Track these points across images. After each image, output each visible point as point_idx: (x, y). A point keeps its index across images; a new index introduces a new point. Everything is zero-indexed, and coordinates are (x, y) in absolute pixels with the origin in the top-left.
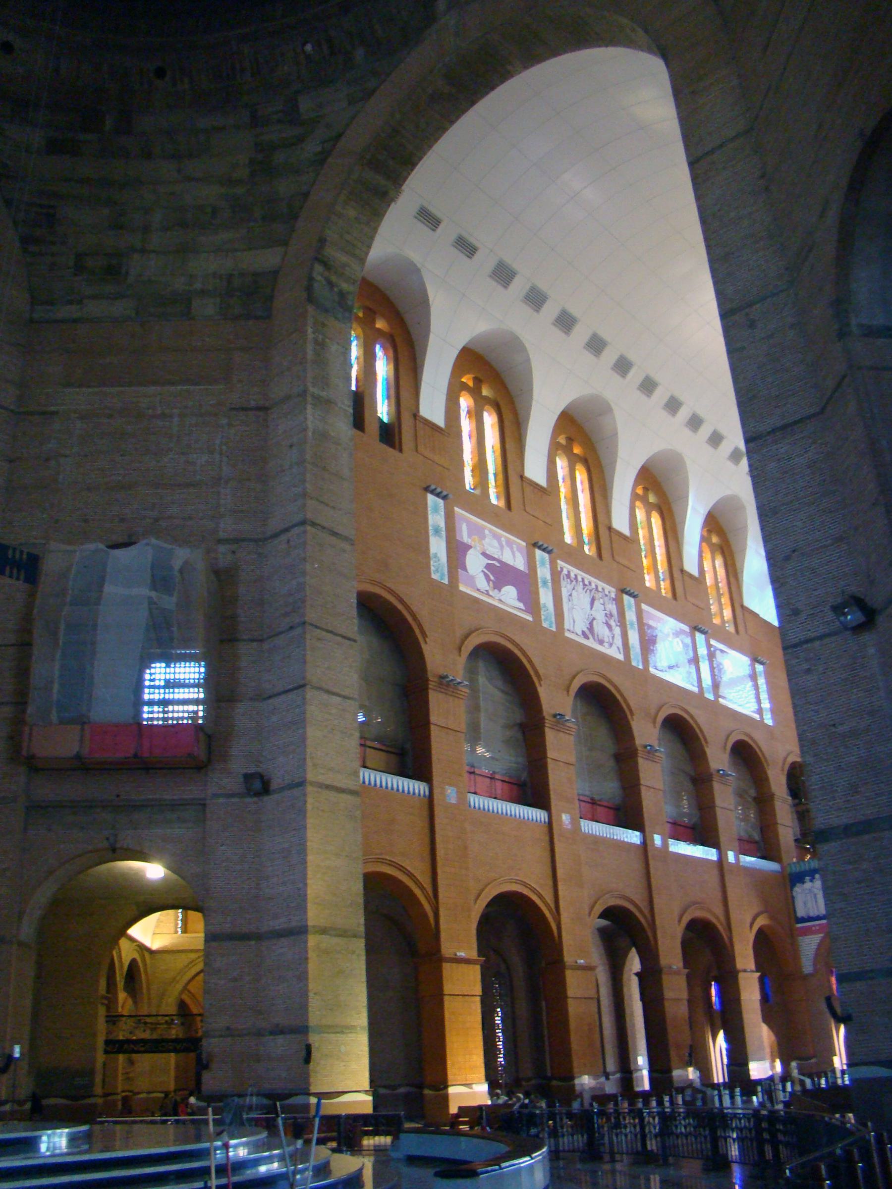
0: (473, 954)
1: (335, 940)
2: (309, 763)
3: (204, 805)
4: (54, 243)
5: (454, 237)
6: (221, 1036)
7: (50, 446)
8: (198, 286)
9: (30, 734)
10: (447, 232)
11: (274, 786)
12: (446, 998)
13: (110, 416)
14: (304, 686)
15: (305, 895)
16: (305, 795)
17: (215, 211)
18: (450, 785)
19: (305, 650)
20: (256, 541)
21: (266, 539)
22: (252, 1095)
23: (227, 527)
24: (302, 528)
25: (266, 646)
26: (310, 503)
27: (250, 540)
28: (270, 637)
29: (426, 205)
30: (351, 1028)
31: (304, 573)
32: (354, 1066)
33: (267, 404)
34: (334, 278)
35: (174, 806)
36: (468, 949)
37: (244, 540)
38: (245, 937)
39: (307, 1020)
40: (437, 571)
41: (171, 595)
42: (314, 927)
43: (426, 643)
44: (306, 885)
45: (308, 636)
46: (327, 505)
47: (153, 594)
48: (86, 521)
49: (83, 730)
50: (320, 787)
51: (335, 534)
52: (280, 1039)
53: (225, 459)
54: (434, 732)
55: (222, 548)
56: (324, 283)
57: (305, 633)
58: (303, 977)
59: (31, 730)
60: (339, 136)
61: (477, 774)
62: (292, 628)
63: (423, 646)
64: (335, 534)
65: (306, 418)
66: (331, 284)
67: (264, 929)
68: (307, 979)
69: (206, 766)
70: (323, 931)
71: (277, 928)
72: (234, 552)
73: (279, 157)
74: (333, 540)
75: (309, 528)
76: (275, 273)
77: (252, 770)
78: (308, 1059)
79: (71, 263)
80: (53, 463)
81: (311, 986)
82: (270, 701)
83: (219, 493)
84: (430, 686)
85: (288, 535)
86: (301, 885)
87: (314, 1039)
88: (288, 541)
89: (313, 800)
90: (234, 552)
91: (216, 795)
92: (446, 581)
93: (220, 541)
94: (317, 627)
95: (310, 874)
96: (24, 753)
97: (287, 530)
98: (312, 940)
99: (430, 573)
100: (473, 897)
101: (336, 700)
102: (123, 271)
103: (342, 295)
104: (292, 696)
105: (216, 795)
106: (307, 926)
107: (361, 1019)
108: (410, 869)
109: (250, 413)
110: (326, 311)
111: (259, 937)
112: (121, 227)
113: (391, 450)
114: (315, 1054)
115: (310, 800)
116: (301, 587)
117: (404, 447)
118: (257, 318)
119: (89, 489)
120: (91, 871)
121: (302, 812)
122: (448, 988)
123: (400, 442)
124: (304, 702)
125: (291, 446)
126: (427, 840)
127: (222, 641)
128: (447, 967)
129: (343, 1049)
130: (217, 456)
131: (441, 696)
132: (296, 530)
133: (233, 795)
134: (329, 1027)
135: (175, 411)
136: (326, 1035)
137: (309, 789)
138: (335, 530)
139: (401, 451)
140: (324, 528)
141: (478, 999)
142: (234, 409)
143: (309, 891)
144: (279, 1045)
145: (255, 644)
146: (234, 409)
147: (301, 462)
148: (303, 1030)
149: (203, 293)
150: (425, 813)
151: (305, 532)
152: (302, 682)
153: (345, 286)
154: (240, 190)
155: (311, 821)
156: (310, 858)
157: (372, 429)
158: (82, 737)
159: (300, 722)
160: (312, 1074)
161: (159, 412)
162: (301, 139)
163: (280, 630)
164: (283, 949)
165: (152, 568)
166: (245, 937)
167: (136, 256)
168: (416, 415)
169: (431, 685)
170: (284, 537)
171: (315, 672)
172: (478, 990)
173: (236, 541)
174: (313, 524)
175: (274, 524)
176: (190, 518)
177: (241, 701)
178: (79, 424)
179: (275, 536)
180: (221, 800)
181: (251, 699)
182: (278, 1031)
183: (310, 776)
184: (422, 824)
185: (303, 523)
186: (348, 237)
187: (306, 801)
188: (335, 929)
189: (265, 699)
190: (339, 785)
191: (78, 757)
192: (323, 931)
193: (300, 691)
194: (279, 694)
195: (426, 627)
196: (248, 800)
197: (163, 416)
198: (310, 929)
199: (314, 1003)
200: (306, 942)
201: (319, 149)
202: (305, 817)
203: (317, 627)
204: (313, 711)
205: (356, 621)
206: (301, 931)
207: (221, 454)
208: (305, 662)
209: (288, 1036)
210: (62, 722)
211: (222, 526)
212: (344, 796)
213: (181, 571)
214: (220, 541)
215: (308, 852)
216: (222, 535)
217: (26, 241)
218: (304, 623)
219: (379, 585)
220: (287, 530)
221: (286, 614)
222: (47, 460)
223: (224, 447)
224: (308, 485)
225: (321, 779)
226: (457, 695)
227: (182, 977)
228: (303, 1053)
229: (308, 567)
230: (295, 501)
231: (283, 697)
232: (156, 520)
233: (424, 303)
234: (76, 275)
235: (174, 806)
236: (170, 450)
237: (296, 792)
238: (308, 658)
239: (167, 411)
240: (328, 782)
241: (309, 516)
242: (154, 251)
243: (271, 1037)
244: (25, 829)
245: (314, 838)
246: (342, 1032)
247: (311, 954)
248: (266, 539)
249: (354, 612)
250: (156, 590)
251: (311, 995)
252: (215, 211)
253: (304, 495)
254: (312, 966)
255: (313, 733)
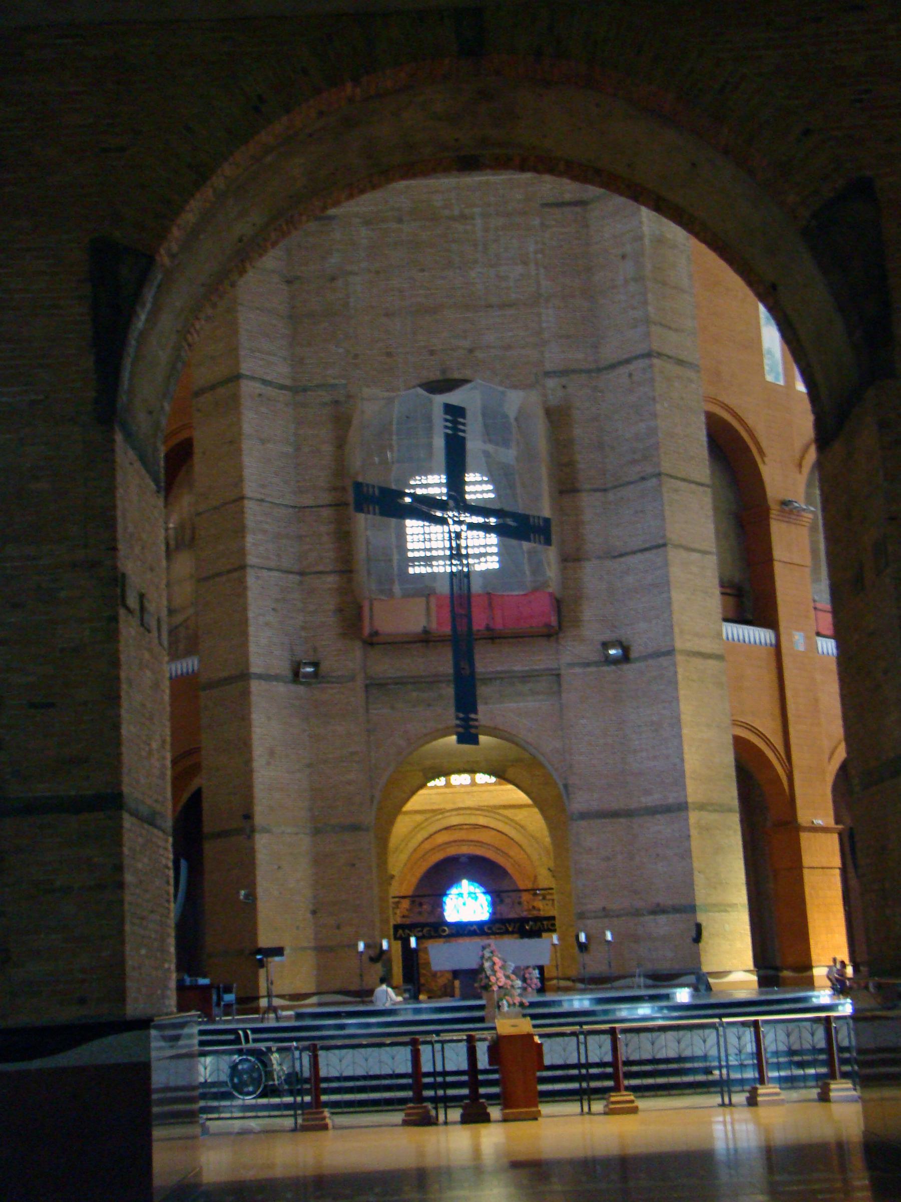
0: (830, 821)
1: (714, 816)
2: (676, 630)
3: (558, 675)
6: (596, 918)
7: (333, 261)
9: (371, 609)
11: (633, 654)
12: (806, 872)
13: (400, 221)
14: (664, 545)
15: (684, 771)
16: (675, 665)
18: (798, 630)
19: (662, 505)
20: (589, 371)
21: (599, 370)
22: (639, 976)
23: (554, 357)
24: (647, 361)
25: (611, 496)
26: (654, 329)
27: (581, 371)
28: (615, 487)
30: (733, 906)
31: (654, 415)
32: (738, 945)
35: (526, 677)
36: (824, 817)
37: (574, 371)
38: (615, 814)
39: (694, 899)
40: (771, 370)
41: (506, 443)
42: (693, 803)
43: (764, 462)
44: (682, 760)
45: (664, 489)
46: (670, 328)
47: (490, 447)
48: (389, 355)
49: (428, 603)
50: (688, 655)
51: (681, 362)
52: (662, 919)
53: (542, 271)
54: (779, 570)
55: (551, 383)
57: (660, 485)
58: (686, 855)
59: (371, 605)
61: (821, 610)
62: (643, 479)
63: (761, 467)
64: (681, 362)
65: (641, 222)
67: (633, 805)
68: (691, 857)
69: (557, 634)
70: (702, 807)
71: (649, 804)
72: (564, 387)
74: (677, 370)
75: (655, 361)
77: (607, 636)
78: (698, 938)
80: (340, 283)
81: (695, 865)
82: (623, 559)
83: (539, 315)
84: (772, 516)
85: (631, 367)
86: (677, 761)
87: (701, 918)
88: (630, 375)
89: (685, 669)
90: (564, 387)
91: (571, 665)
92: (781, 382)
93: (548, 374)
94: (671, 477)
95: (686, 748)
96: (367, 631)
97: (627, 361)
98: (693, 817)
99: (763, 375)
100: (827, 756)
101: (695, 556)
104: (648, 555)
105: (571, 665)
106: (686, 803)
107: (740, 896)
108: (761, 730)
109: (567, 210)
111: (629, 814)
114: (705, 934)
115: (680, 670)
116: (652, 432)
119: (387, 315)
120: (428, 747)
121: (673, 683)
122: (807, 860)
124: (666, 564)
125: (624, 257)
126: (776, 694)
127: (561, 492)
128: (804, 836)
129: (727, 927)
130: (532, 266)
131: (784, 526)
132: (641, 363)
133: (588, 665)
134: (715, 905)
135: (475, 210)
136: (710, 914)
137: (679, 658)
138: (680, 357)
140: (669, 357)
141: (838, 872)
142: (547, 205)
143: (687, 767)
144: (662, 925)
145: (598, 494)
146: (547, 205)
147: (639, 279)
148: (691, 909)
150: (773, 664)
151: (651, 366)
152: (661, 542)
155: (682, 692)
156: (685, 731)
158: (428, 608)
159: (663, 585)
160: (702, 954)
161: (456, 213)
163: (627, 479)
164: (659, 827)
165: (484, 415)
166: (615, 814)
169: (774, 513)
170: (623, 370)
171: (675, 530)
172: (837, 862)
173: (564, 373)
174: (659, 355)
175: (609, 353)
176: (509, 347)
177: (588, 560)
178: (364, 232)
179: (613, 367)
180: (578, 670)
181: (599, 558)
182: (658, 910)
183: (679, 644)
184: (770, 677)
185: (649, 355)
187: (676, 672)
188: (712, 804)
189: (615, 557)
190: (703, 650)
191: (426, 631)
192: (702, 807)
193: (660, 550)
194: (634, 552)
195: (764, 444)
196: (606, 668)
197: (463, 217)
198: (690, 806)
199: (699, 880)
200: (687, 819)
202: (676, 689)
203: (671, 477)
204: (676, 572)
205: (707, 463)
206: (682, 807)
207: (537, 264)
208: (663, 519)
209: (671, 916)
210: (407, 595)
211: (547, 355)
212: (711, 663)
213: (516, 419)
214: (548, 374)
215: (683, 725)
216: (548, 367)
218: (659, 475)
219: (714, 401)
220: (627, 361)
221: (634, 462)
222: (333, 279)
223: (540, 256)
224: (650, 308)
225: (688, 646)
226: (798, 522)
227: (407, 844)
228: (693, 934)
229: (658, 407)
230: (636, 327)
231: (639, 556)
232: (471, 351)
235: (526, 677)
236: (475, 262)
237: (664, 661)
238: (667, 514)
239: (466, 211)
240: (696, 648)
241: (655, 346)
243: (652, 917)
244: (367, 710)
245: (687, 709)
246: (726, 911)
247: (694, 832)
248: (599, 370)
249: (705, 453)
250: (490, 441)
251: (696, 873)
253: (647, 321)
254: (695, 843)
255: (677, 596)
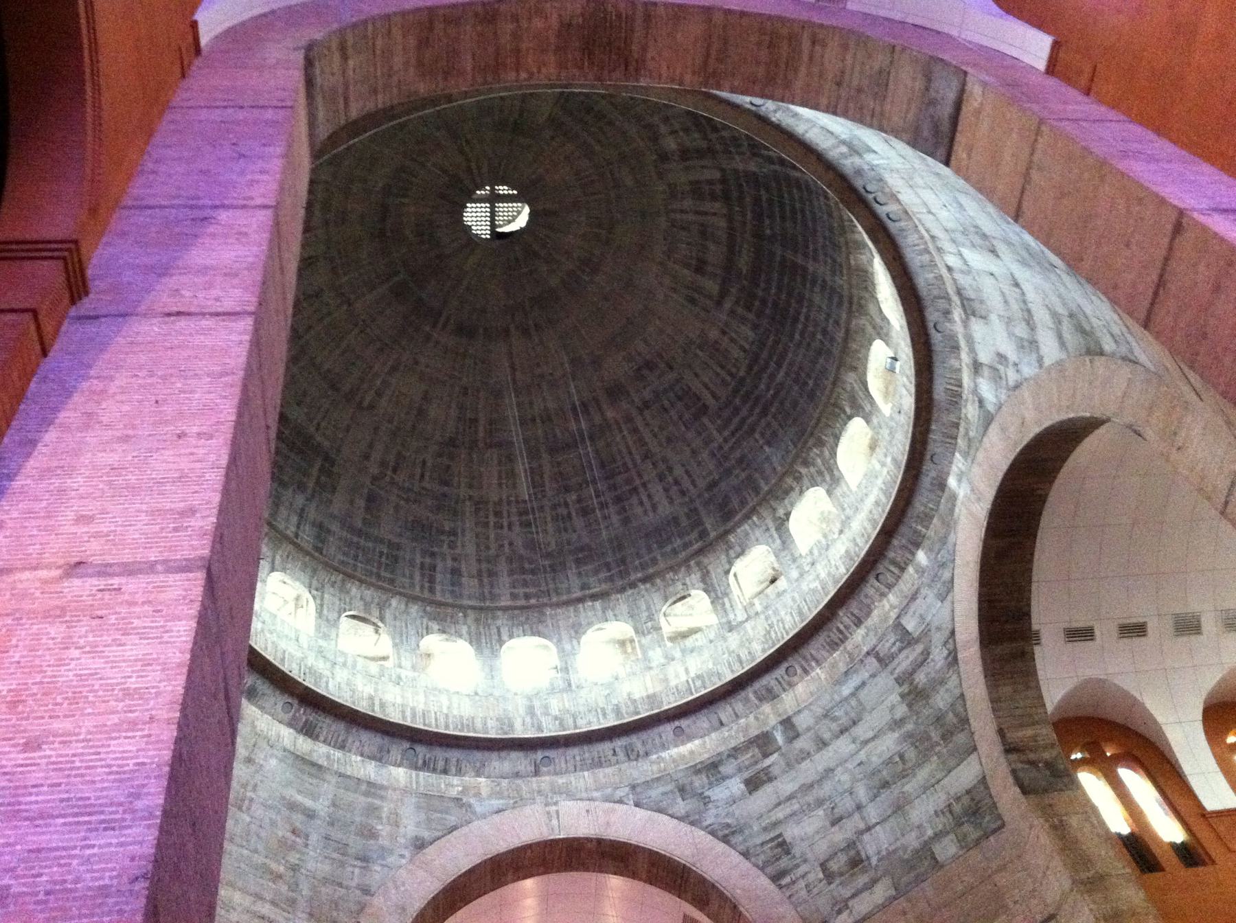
4: (797, 866)
5: (1115, 632)
8: (930, 832)
10: (1105, 632)
17: (902, 757)
29: (1067, 625)
33: (1051, 910)
34: (1032, 756)
56: (1027, 766)
60: (953, 633)
66: (1033, 763)
73: (921, 678)
76: (983, 780)
79: (821, 875)
102: (864, 856)
103: (1049, 765)
110: (1046, 791)
112: (840, 819)
113: (1201, 869)
117: (1213, 854)
118: (994, 831)
123: (1210, 857)
139: (1213, 862)
149: (938, 836)
153: (1046, 755)
154: (909, 727)
157: (1171, 861)
162: (926, 653)
167: (866, 837)
168: (1204, 815)
186: (1018, 712)
201: (946, 652)
217: (776, 878)
233: (1135, 704)
234: (830, 883)
242: (878, 823)
252: (902, 757)
